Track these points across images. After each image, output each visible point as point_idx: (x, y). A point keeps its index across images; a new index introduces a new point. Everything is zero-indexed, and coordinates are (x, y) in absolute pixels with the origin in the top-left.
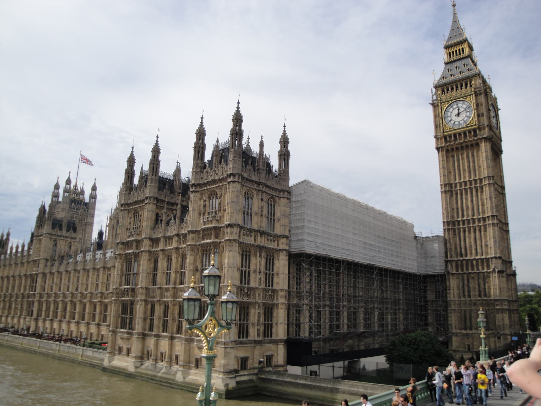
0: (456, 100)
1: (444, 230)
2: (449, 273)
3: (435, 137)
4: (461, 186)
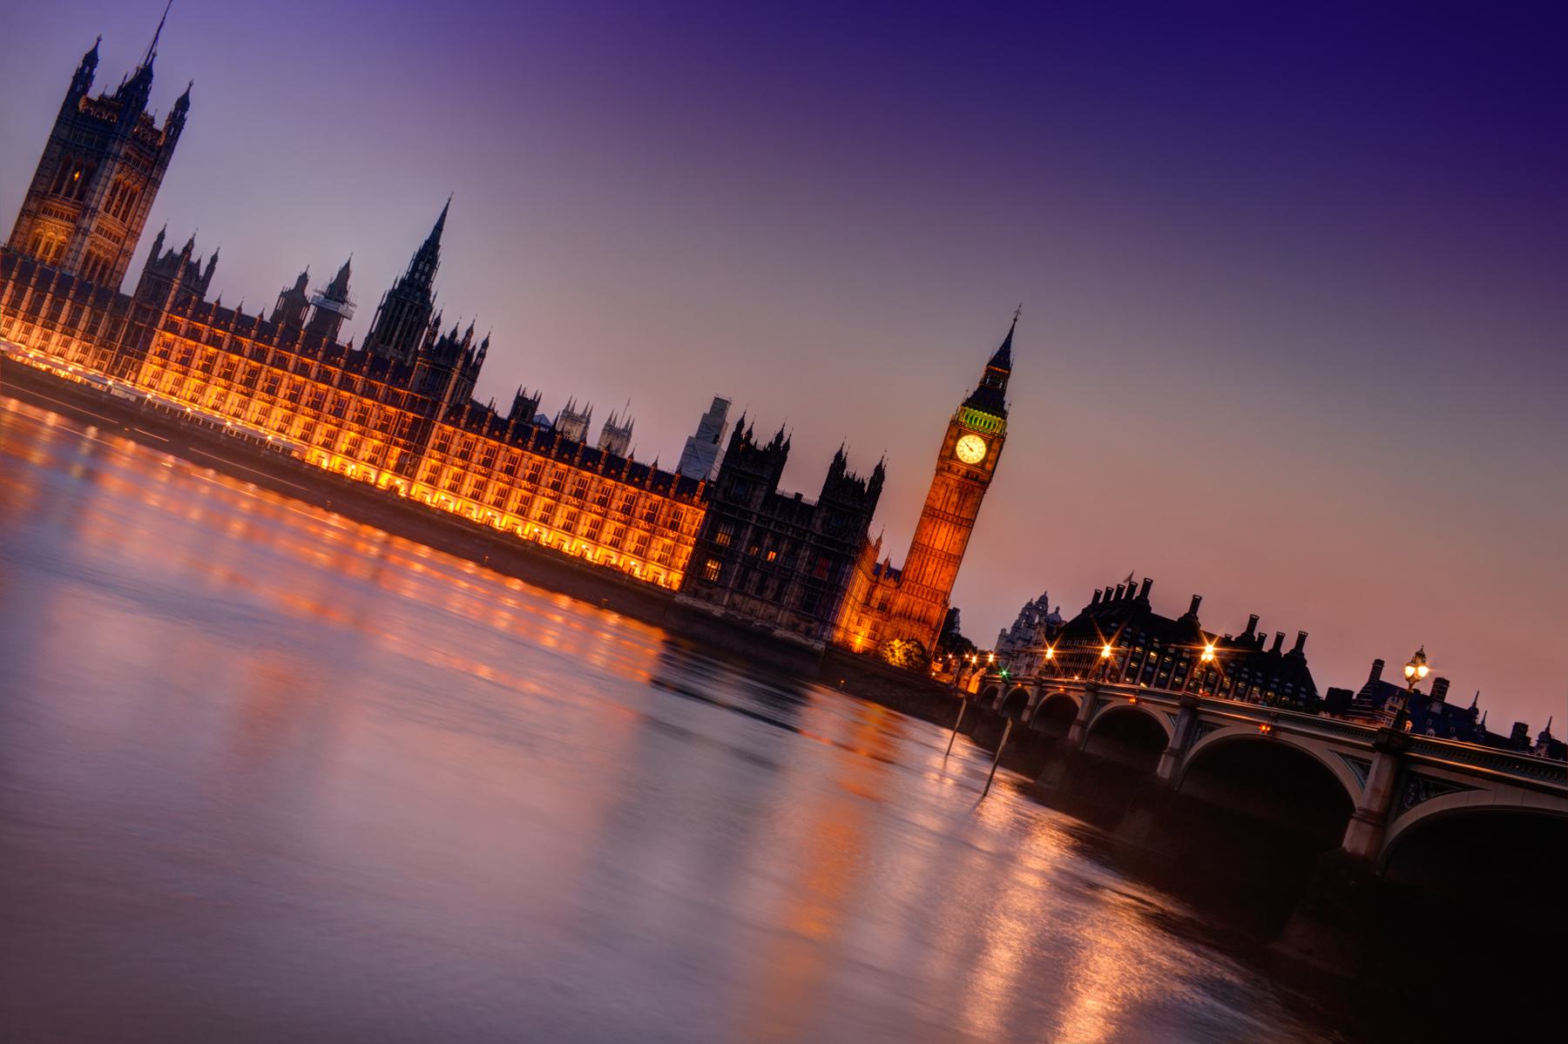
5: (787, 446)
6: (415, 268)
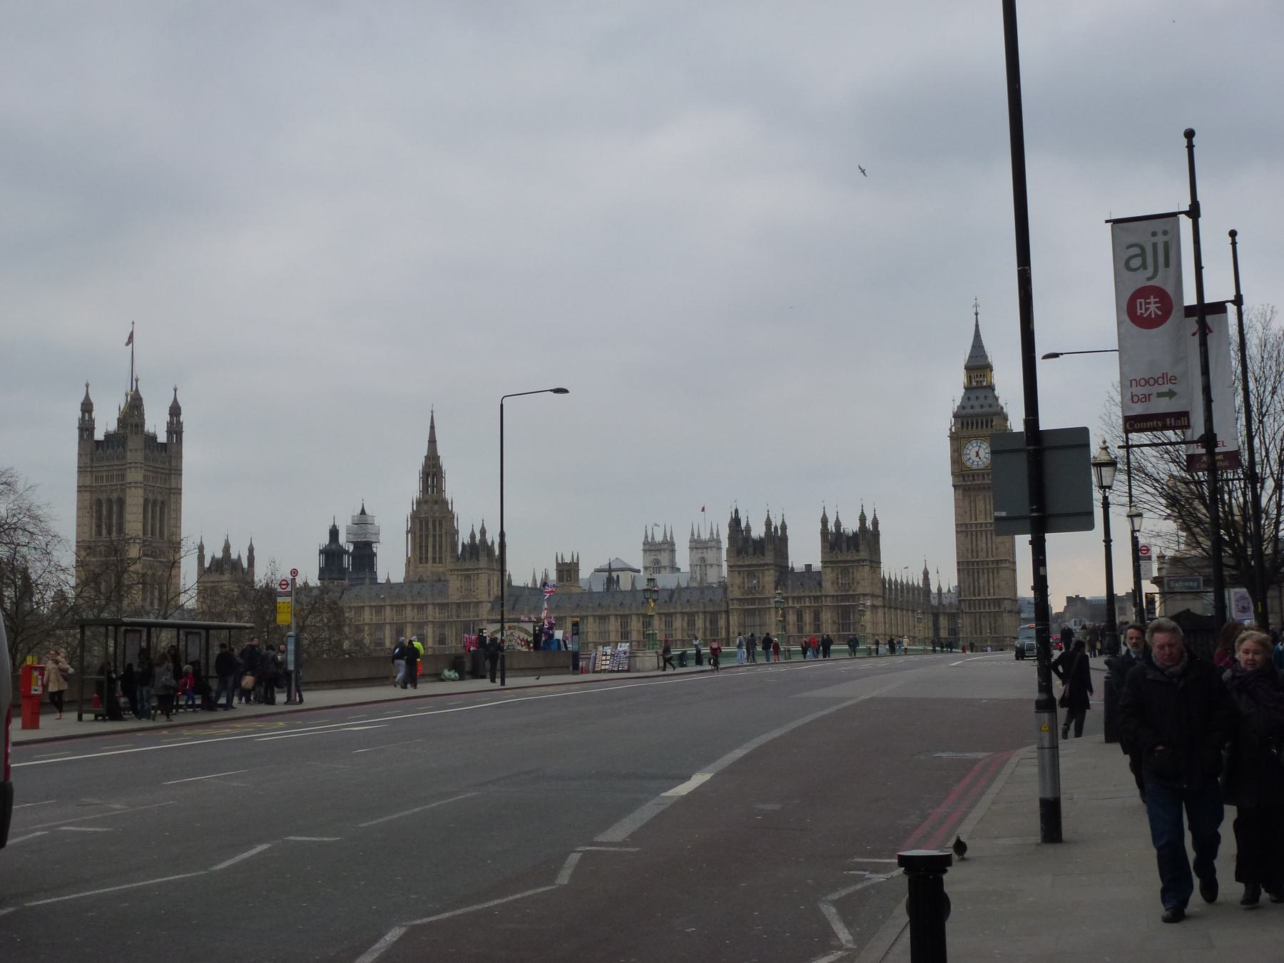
0: (976, 437)
1: (958, 570)
2: (962, 612)
3: (952, 474)
4: (976, 528)
5: (784, 527)
6: (425, 489)
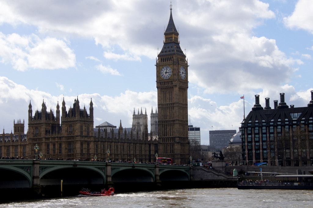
4: (166, 105)
